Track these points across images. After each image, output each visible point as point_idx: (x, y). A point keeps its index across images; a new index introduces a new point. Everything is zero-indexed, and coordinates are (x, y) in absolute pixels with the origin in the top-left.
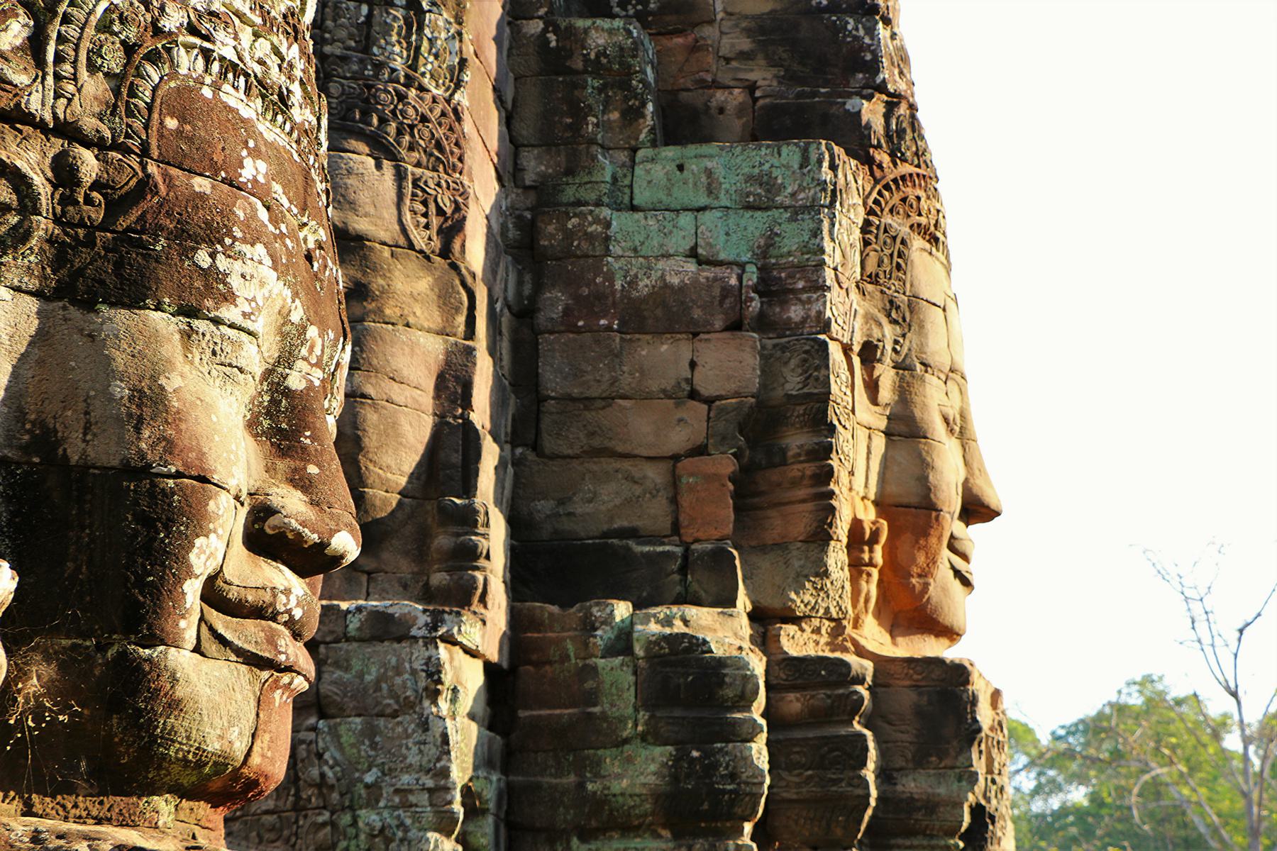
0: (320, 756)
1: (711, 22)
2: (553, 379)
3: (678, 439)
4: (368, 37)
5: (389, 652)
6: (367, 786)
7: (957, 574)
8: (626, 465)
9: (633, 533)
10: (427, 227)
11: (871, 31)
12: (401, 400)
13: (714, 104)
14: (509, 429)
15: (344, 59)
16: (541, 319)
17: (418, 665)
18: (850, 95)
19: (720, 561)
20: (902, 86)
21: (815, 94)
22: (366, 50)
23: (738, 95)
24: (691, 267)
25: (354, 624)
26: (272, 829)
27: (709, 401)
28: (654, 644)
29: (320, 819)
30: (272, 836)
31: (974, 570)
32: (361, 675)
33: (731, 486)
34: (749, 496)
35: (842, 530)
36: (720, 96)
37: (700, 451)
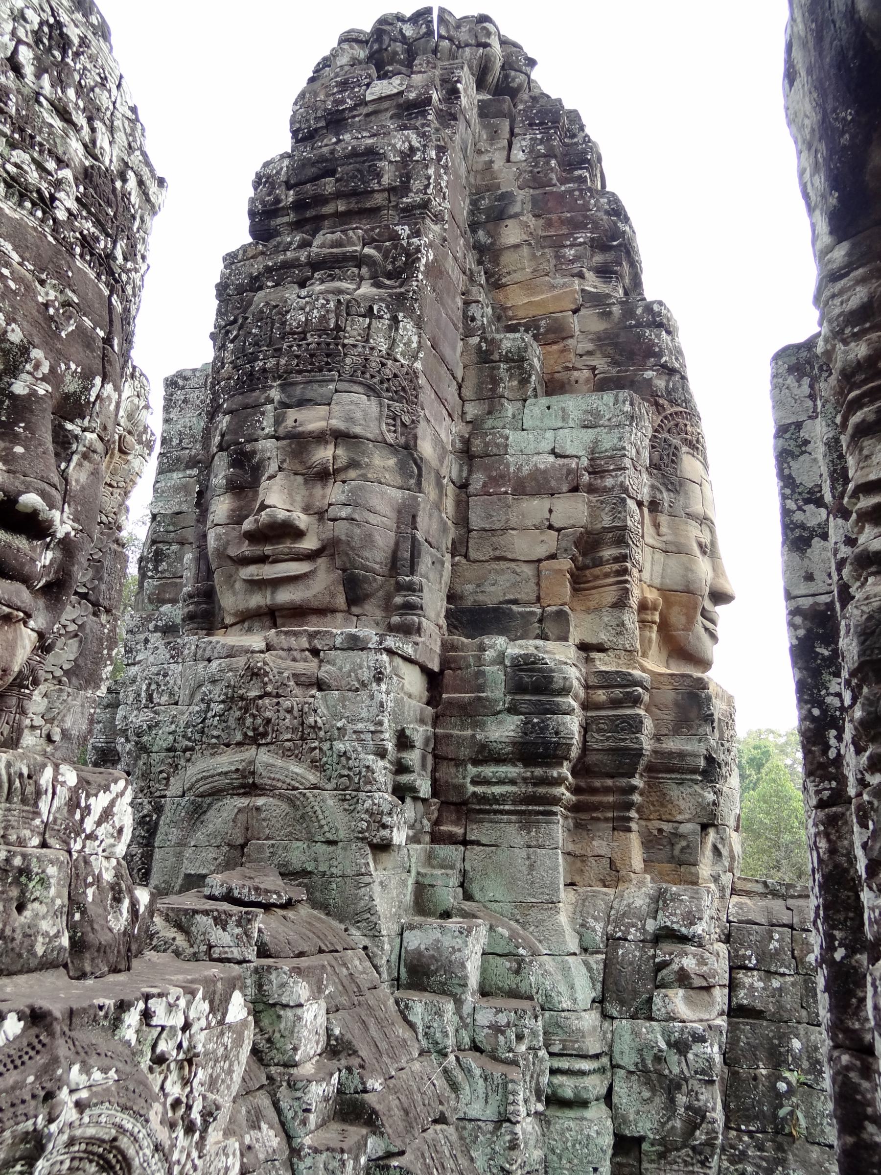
0: (315, 711)
1: (572, 337)
2: (476, 520)
3: (541, 551)
4: (368, 335)
5: (357, 657)
6: (338, 729)
7: (706, 629)
8: (513, 565)
9: (515, 602)
10: (395, 432)
11: (658, 336)
12: (375, 522)
13: (573, 379)
14: (450, 546)
15: (355, 346)
16: (471, 489)
17: (371, 664)
18: (647, 370)
19: (561, 617)
20: (677, 365)
21: (627, 371)
22: (367, 341)
23: (586, 373)
24: (552, 458)
25: (338, 641)
26: (289, 750)
27: (559, 530)
28: (514, 658)
29: (313, 745)
30: (289, 753)
31: (720, 630)
32: (340, 669)
33: (568, 576)
34: (579, 582)
35: (634, 602)
36: (576, 374)
37: (553, 557)
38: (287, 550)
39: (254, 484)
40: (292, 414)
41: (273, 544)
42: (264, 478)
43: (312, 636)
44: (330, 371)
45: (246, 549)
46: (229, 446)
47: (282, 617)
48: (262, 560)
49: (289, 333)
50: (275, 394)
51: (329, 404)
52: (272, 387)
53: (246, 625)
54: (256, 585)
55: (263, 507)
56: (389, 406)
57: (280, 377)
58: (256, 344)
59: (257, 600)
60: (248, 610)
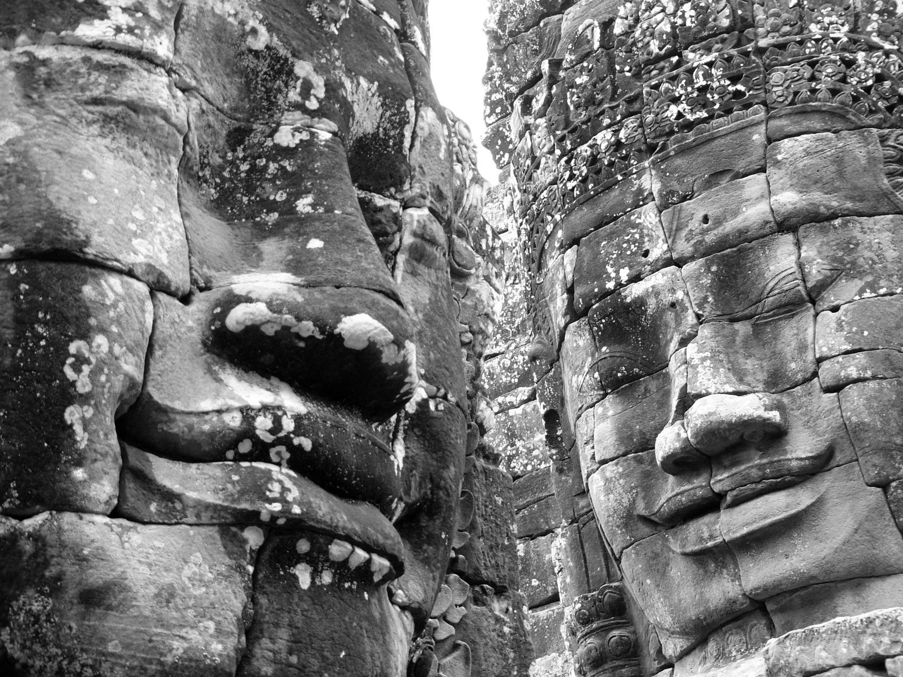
38: (755, 473)
39: (657, 366)
40: (696, 209)
41: (726, 468)
42: (673, 346)
43: (855, 634)
44: (747, 106)
45: (671, 491)
46: (588, 307)
47: (782, 610)
48: (711, 504)
49: (648, 63)
50: (650, 183)
51: (763, 170)
52: (640, 174)
53: (712, 646)
54: (716, 557)
55: (687, 401)
56: (883, 139)
57: (651, 149)
58: (591, 101)
59: (722, 590)
60: (709, 613)
